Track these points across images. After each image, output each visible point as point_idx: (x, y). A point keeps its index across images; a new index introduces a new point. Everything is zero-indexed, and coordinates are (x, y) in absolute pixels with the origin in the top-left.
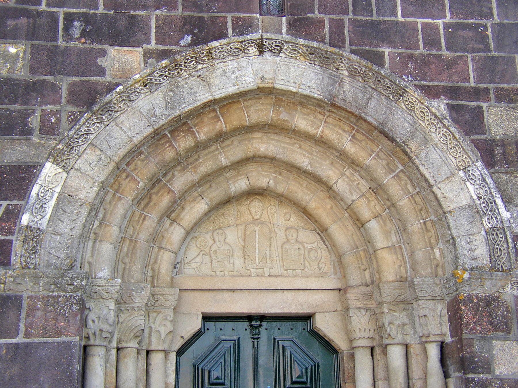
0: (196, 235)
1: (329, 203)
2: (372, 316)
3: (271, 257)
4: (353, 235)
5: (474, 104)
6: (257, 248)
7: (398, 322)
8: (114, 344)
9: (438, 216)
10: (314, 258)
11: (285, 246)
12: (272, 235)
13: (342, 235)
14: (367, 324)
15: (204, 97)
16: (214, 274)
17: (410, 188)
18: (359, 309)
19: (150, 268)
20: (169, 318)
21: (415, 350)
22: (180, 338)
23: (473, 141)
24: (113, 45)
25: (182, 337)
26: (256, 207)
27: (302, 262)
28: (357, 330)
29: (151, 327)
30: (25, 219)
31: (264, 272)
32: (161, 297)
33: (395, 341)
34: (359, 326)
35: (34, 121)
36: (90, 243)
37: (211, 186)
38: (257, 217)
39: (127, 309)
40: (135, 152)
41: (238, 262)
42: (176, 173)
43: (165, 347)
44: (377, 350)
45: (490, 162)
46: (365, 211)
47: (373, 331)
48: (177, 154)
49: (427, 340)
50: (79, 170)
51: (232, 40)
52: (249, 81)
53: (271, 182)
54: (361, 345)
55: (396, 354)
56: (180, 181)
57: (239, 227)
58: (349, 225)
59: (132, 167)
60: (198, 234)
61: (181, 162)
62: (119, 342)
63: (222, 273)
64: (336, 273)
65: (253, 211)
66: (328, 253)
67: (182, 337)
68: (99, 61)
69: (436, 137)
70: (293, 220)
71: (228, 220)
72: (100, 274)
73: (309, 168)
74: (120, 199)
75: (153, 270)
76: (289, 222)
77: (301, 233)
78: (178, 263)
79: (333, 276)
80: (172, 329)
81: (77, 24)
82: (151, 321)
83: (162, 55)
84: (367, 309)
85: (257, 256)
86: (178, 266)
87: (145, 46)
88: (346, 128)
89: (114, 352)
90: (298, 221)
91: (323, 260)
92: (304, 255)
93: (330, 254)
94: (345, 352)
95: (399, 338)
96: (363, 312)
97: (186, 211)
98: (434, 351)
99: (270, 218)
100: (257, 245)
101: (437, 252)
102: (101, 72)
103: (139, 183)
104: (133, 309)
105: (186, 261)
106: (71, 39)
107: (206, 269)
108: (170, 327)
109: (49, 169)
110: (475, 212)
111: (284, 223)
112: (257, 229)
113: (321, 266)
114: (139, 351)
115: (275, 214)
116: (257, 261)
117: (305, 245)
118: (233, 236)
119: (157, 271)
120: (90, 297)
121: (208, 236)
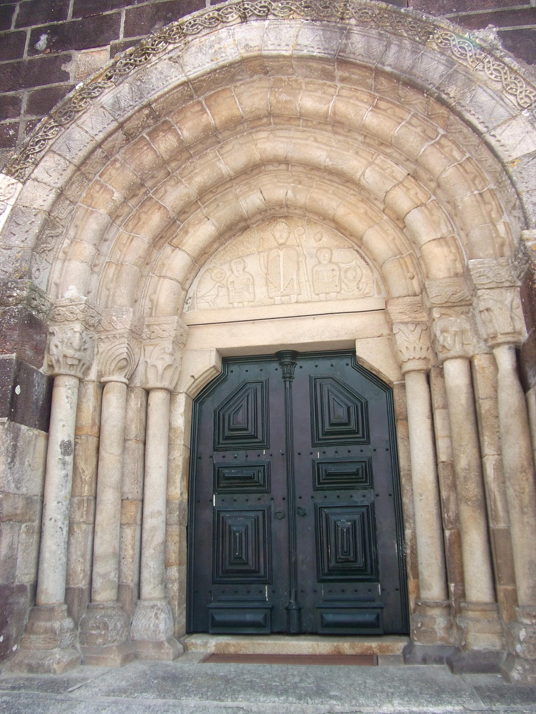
0: (211, 266)
1: (362, 208)
2: (424, 332)
3: (299, 283)
4: (394, 239)
6: (282, 274)
7: (454, 329)
10: (352, 278)
11: (315, 269)
12: (300, 259)
13: (381, 241)
14: (417, 342)
15: (177, 78)
16: (231, 306)
17: (456, 154)
18: (406, 323)
19: (147, 299)
20: (167, 350)
21: (480, 362)
22: (189, 378)
24: (79, 49)
25: (193, 377)
27: (337, 284)
28: (404, 350)
29: (146, 362)
31: (290, 299)
32: (157, 327)
33: (452, 353)
34: (406, 344)
36: (58, 265)
37: (218, 205)
38: (281, 241)
39: (107, 338)
41: (261, 292)
42: (168, 188)
44: (433, 374)
46: (402, 200)
47: (426, 349)
48: (158, 157)
49: (494, 342)
50: (35, 180)
52: (231, 54)
53: (290, 192)
54: (411, 368)
55: (455, 373)
56: (174, 196)
57: (261, 254)
58: (389, 228)
59: (106, 177)
60: (214, 265)
61: (167, 168)
62: (100, 375)
63: (241, 305)
64: (379, 293)
65: (277, 235)
66: (369, 271)
67: (193, 377)
70: (325, 240)
71: (248, 248)
73: (328, 162)
74: (92, 212)
75: (151, 301)
76: (321, 242)
77: (336, 253)
78: (190, 298)
79: (376, 296)
80: (170, 363)
82: (147, 355)
84: (417, 324)
85: (282, 282)
86: (190, 301)
88: (365, 97)
90: (332, 240)
91: (363, 280)
92: (340, 275)
93: (372, 271)
94: (395, 383)
95: (457, 350)
96: (411, 327)
97: (190, 235)
98: (506, 359)
99: (298, 240)
100: (282, 270)
101: (501, 229)
102: (65, 76)
103: (113, 193)
104: (114, 337)
105: (199, 294)
106: (37, 52)
107: (222, 302)
108: (168, 360)
111: (315, 244)
112: (281, 253)
113: (361, 286)
114: (129, 388)
115: (304, 236)
116: (282, 287)
117: (341, 265)
118: (254, 265)
119: (155, 302)
120: (53, 320)
121: (226, 267)
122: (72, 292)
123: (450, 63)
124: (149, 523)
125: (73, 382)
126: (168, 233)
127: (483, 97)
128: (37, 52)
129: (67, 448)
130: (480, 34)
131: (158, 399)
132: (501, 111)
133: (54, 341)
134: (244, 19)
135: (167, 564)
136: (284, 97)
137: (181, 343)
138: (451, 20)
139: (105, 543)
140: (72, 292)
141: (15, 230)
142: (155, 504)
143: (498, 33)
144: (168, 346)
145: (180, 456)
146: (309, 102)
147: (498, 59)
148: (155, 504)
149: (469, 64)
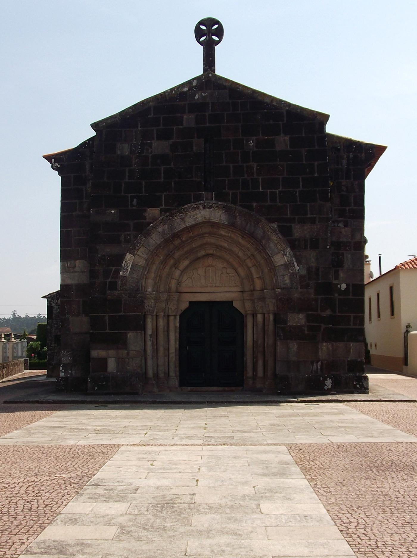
5: (288, 224)
8: (155, 313)
9: (273, 268)
15: (183, 226)
18: (248, 300)
40: (158, 247)
43: (174, 314)
44: (254, 315)
45: (293, 248)
51: (194, 205)
52: (200, 220)
69: (274, 238)
72: (148, 290)
74: (154, 263)
81: (135, 200)
83: (166, 211)
87: (161, 207)
89: (155, 317)
101: (274, 280)
102: (145, 218)
106: (134, 206)
108: (175, 307)
109: (128, 256)
110: (287, 266)
122: (150, 289)
123: (264, 232)
124: (171, 356)
125: (150, 317)
127: (272, 245)
128: (134, 206)
129: (151, 336)
130: (273, 225)
131: (172, 318)
132: (276, 250)
133: (146, 305)
134: (204, 208)
135: (176, 367)
136: (215, 230)
139: (161, 361)
140: (150, 289)
142: (172, 350)
143: (278, 226)
146: (223, 233)
147: (277, 234)
148: (172, 350)
149: (269, 233)
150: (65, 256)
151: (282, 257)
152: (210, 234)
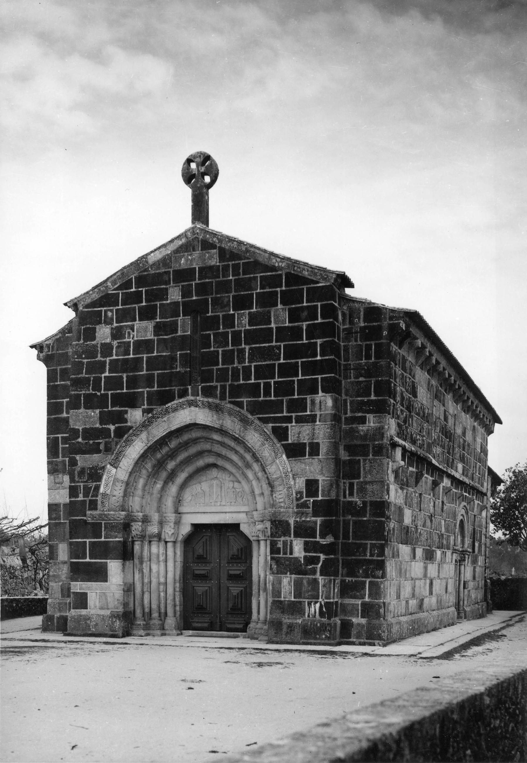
23: (282, 445)
26: (214, 472)
30: (102, 490)
35: (102, 447)
56: (171, 465)
59: (145, 462)
68: (126, 416)
87: (143, 407)
102: (126, 421)
108: (173, 531)
126: (172, 476)
137: (178, 523)
138: (259, 419)
141: (116, 488)
144: (172, 525)
145: (179, 565)
150: (53, 469)
151: (280, 464)
152: (208, 439)
